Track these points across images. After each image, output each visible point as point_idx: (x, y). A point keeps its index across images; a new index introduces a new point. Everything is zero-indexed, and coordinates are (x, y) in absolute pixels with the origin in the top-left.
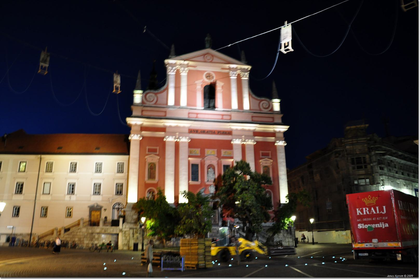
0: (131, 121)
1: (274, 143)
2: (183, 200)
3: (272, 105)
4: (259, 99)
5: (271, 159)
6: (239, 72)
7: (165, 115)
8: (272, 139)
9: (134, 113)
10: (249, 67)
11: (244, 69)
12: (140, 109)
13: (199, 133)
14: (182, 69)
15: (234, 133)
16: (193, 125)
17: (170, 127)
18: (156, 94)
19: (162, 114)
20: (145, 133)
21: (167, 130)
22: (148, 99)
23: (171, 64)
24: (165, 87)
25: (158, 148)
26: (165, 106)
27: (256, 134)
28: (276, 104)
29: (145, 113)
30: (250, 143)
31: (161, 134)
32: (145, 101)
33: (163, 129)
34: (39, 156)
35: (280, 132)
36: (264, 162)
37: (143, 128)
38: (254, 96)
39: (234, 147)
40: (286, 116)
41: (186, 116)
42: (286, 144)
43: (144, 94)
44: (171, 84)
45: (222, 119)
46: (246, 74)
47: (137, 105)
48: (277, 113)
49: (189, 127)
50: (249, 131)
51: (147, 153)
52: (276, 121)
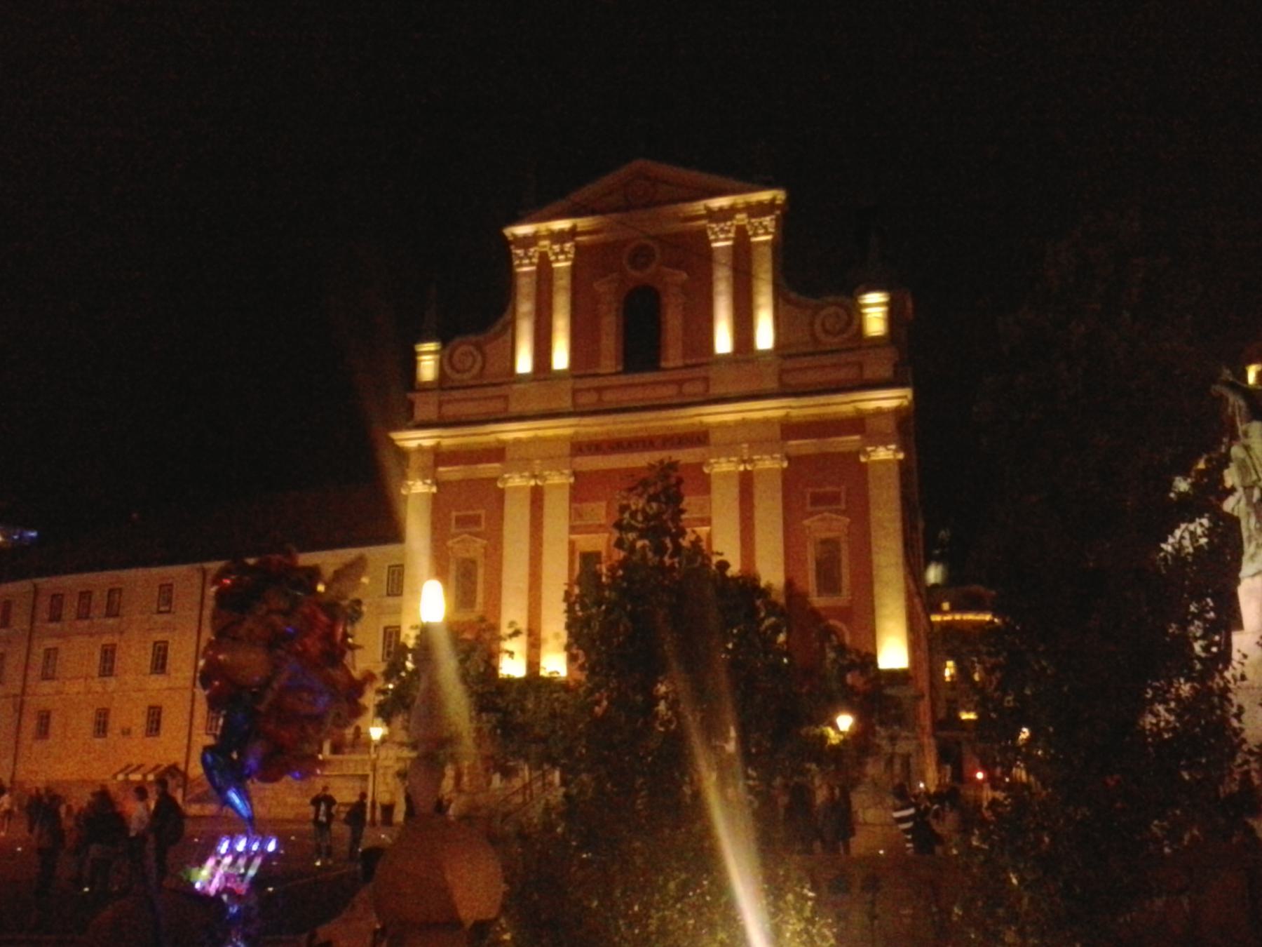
0: (413, 439)
1: (858, 453)
2: (555, 664)
3: (861, 316)
4: (814, 302)
5: (844, 513)
6: (741, 218)
7: (506, 410)
8: (851, 441)
9: (420, 414)
10: (779, 195)
11: (760, 203)
12: (433, 398)
13: (605, 453)
14: (557, 248)
15: (715, 437)
16: (583, 430)
17: (518, 442)
18: (479, 346)
19: (497, 405)
20: (449, 472)
21: (509, 455)
22: (459, 366)
23: (525, 237)
24: (507, 316)
25: (482, 512)
26: (506, 380)
27: (790, 429)
28: (875, 311)
29: (450, 410)
30: (770, 464)
31: (487, 469)
32: (448, 371)
33: (497, 453)
34: (198, 565)
35: (879, 413)
36: (825, 525)
37: (440, 457)
38: (793, 295)
39: (714, 486)
40: (908, 352)
41: (567, 404)
42: (901, 456)
43: (447, 352)
44: (525, 307)
45: (680, 394)
46: (768, 221)
47: (426, 388)
48: (875, 342)
49: (571, 437)
50: (766, 422)
51: (453, 530)
52: (868, 374)
